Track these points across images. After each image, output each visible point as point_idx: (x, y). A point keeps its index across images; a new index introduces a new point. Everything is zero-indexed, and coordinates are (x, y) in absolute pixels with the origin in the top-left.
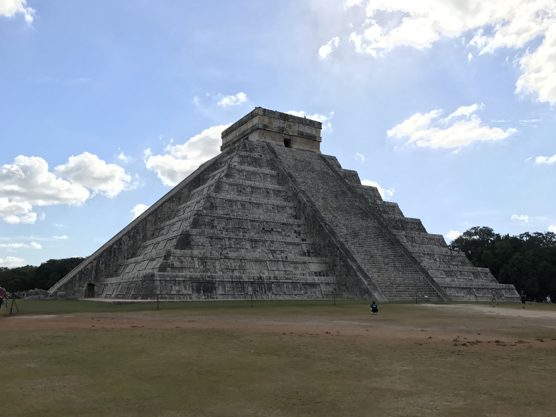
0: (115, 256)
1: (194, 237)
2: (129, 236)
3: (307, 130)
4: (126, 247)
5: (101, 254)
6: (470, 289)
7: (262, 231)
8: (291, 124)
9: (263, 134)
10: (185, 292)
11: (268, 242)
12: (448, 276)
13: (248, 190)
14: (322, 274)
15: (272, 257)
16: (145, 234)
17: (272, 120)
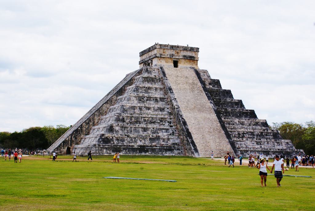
0: (79, 133)
2: (86, 123)
3: (189, 54)
4: (85, 129)
5: (73, 132)
6: (270, 152)
7: (149, 123)
8: (179, 51)
9: (160, 60)
11: (151, 129)
12: (258, 144)
13: (145, 99)
14: (177, 144)
15: (151, 136)
16: (94, 122)
17: (165, 51)
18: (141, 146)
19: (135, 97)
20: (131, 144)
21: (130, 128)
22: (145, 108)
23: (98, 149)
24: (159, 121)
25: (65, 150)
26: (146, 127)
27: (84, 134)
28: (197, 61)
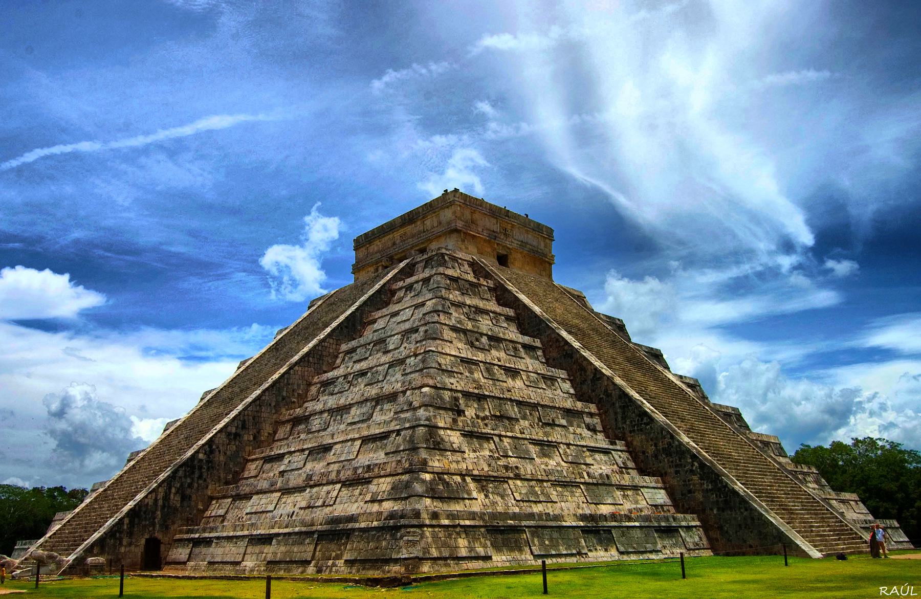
0: (200, 477)
1: (442, 432)
3: (531, 238)
9: (463, 241)
10: (481, 551)
13: (484, 340)
14: (665, 508)
15: (586, 477)
16: (259, 432)
18: (583, 517)
19: (454, 329)
20: (537, 509)
21: (496, 439)
22: (503, 372)
23: (435, 536)
24: (564, 422)
25: (137, 550)
26: (545, 439)
27: (219, 481)
28: (550, 264)
